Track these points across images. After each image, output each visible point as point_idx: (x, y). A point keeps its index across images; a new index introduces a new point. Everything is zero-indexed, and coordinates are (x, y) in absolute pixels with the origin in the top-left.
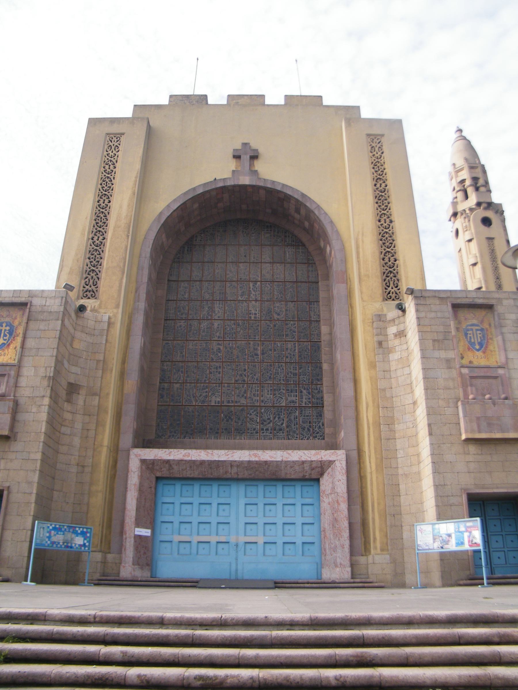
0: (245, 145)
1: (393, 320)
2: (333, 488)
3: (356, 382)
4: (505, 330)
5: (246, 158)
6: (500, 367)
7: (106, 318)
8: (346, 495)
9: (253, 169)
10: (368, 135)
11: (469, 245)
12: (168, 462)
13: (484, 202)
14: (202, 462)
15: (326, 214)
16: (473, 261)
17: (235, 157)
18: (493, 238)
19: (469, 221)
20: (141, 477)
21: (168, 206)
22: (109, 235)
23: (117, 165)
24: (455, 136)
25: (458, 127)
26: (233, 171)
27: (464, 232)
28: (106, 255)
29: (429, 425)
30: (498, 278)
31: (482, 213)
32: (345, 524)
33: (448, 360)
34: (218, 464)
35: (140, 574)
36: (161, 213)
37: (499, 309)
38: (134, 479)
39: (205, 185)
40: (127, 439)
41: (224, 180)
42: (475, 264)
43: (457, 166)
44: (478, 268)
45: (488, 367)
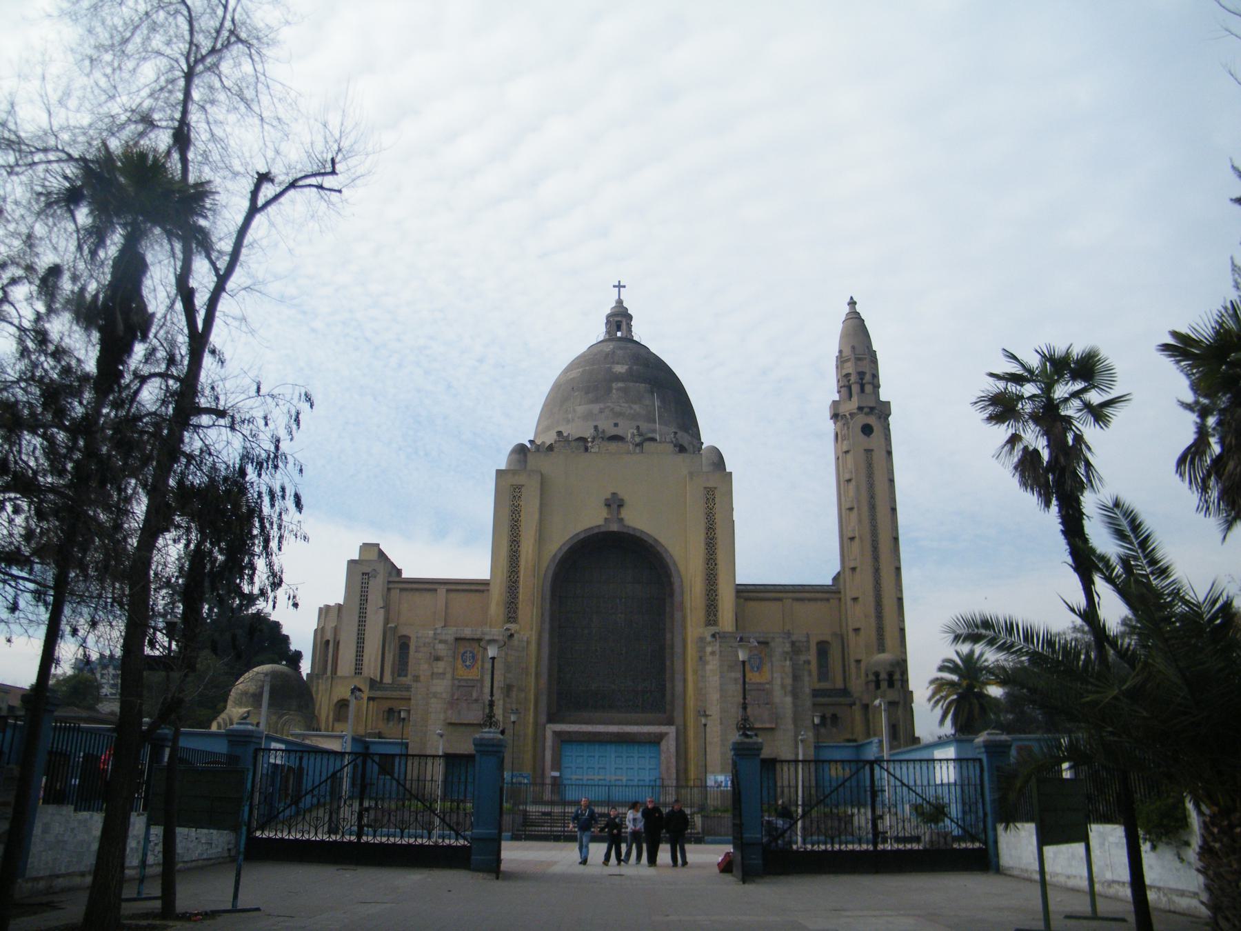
0: (614, 494)
1: (710, 643)
2: (668, 749)
3: (685, 680)
4: (774, 659)
5: (615, 506)
6: (768, 683)
7: (525, 639)
8: (675, 754)
9: (620, 517)
10: (705, 488)
12: (569, 732)
14: (590, 733)
15: (671, 556)
16: (847, 477)
17: (606, 505)
19: (848, 428)
20: (553, 742)
21: (560, 549)
22: (522, 574)
23: (522, 513)
24: (847, 309)
25: (852, 298)
26: (606, 519)
27: (843, 440)
28: (521, 590)
29: (721, 719)
31: (862, 419)
32: (674, 771)
33: (736, 680)
34: (599, 733)
35: (556, 798)
36: (555, 555)
37: (772, 644)
38: (549, 743)
39: (585, 530)
40: (543, 718)
41: (599, 526)
42: (849, 481)
43: (844, 354)
44: (852, 485)
45: (761, 684)
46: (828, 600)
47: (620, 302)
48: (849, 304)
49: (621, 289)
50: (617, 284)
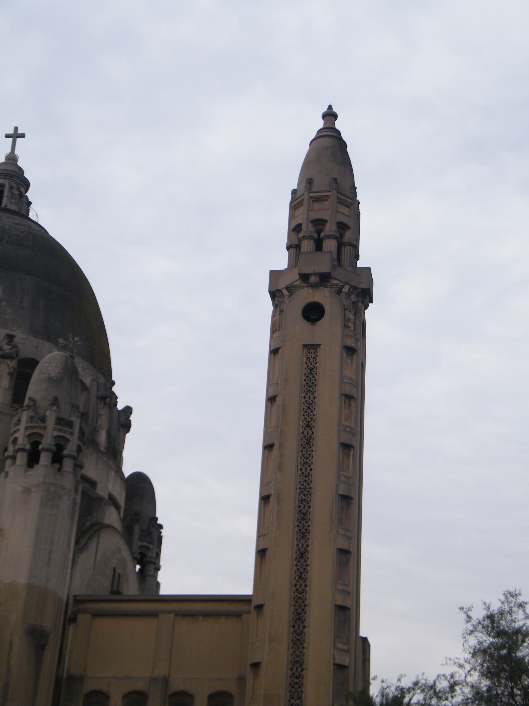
11: (274, 359)
13: (316, 274)
18: (319, 345)
25: (330, 107)
30: (308, 426)
46: (238, 615)
47: (12, 158)
48: (324, 116)
49: (18, 139)
50: (20, 132)
